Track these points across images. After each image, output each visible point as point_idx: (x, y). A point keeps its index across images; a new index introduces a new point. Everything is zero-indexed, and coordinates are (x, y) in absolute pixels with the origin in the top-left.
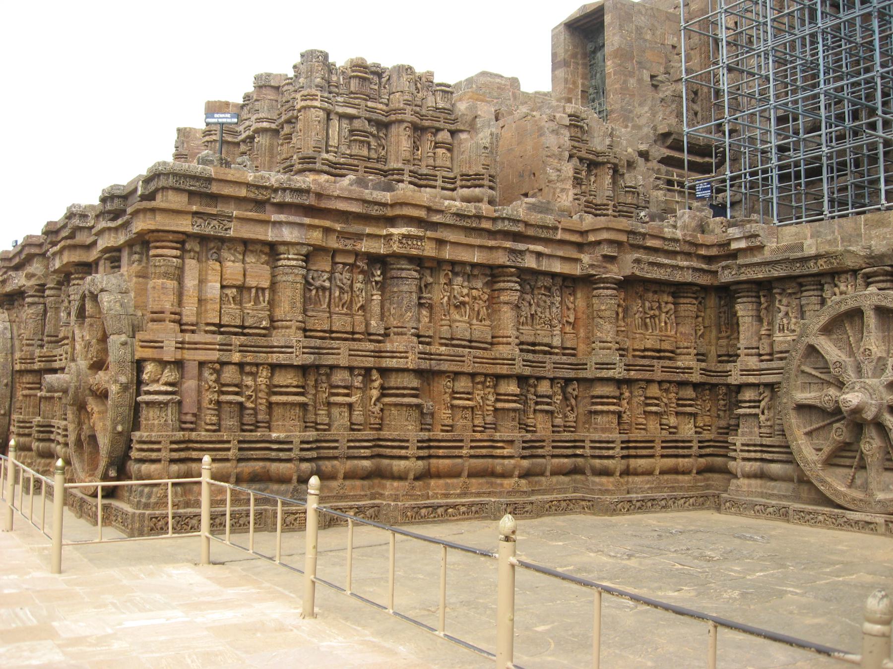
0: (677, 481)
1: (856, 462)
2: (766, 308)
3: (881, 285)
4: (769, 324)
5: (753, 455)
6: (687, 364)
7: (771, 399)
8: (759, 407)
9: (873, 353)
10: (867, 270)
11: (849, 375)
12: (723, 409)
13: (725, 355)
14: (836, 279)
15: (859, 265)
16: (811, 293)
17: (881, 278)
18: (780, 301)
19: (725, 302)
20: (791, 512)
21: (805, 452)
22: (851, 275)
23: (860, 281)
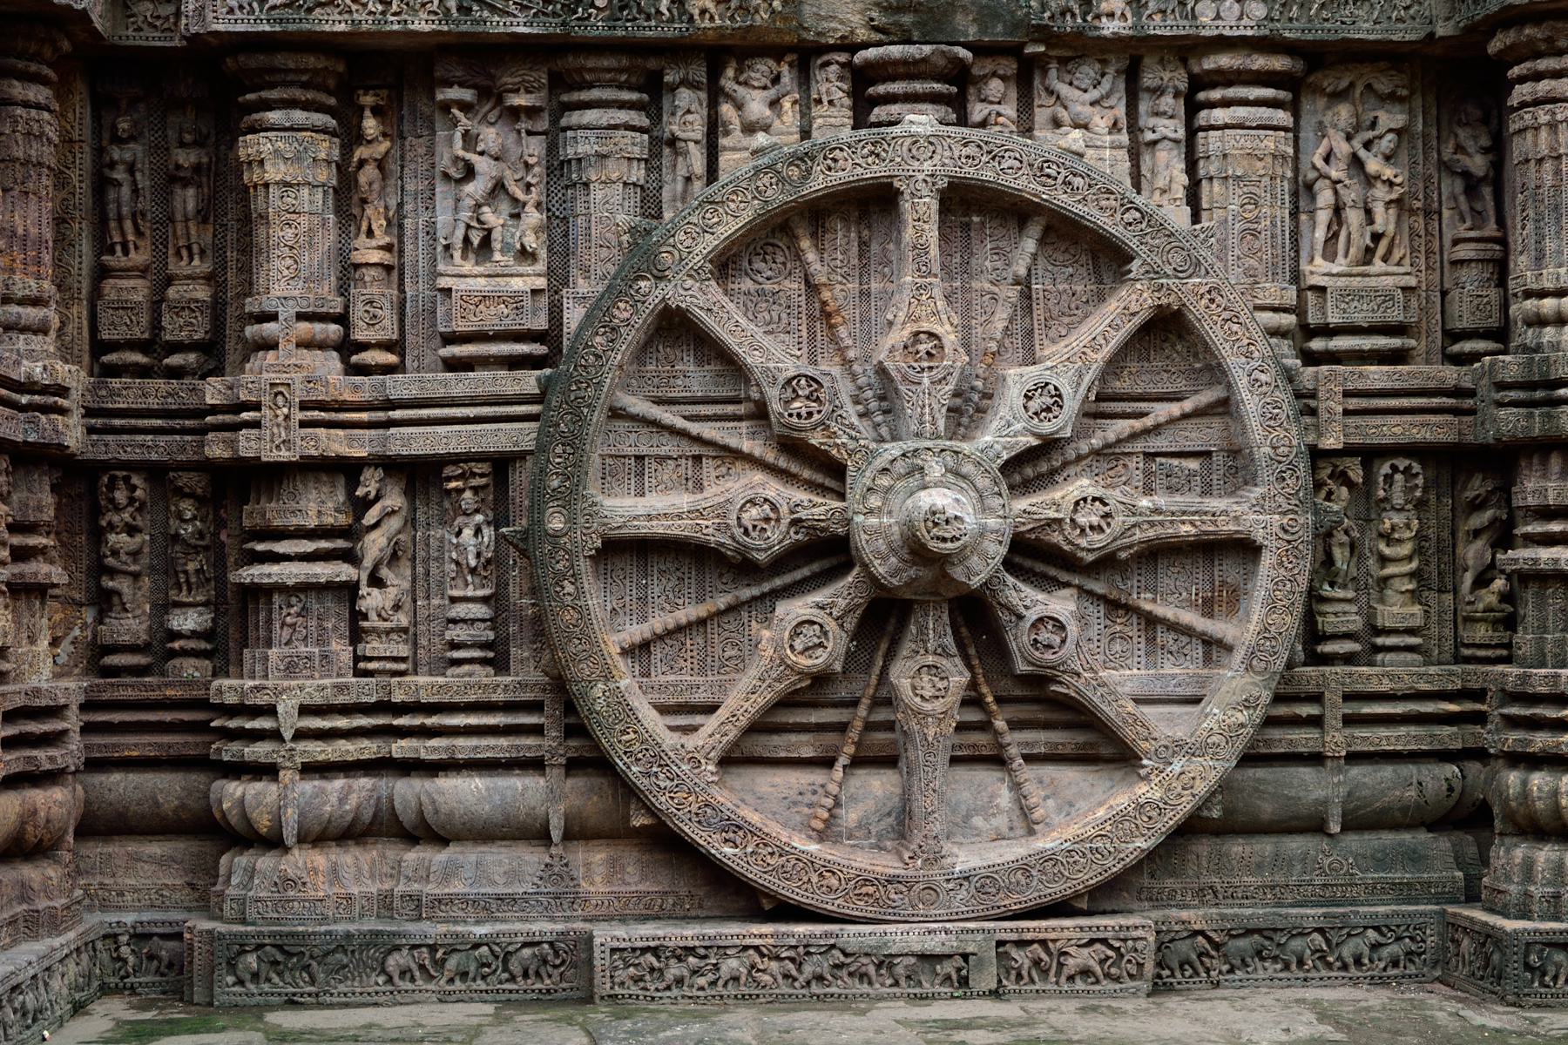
0: (25, 892)
2: (381, 164)
6: (35, 369)
7: (411, 522)
8: (350, 557)
10: (896, 51)
11: (852, 427)
12: (133, 568)
13: (132, 345)
14: (730, 73)
15: (843, 30)
16: (623, 116)
18: (470, 140)
19: (135, 124)
20: (600, 960)
22: (791, 65)
23: (831, 84)
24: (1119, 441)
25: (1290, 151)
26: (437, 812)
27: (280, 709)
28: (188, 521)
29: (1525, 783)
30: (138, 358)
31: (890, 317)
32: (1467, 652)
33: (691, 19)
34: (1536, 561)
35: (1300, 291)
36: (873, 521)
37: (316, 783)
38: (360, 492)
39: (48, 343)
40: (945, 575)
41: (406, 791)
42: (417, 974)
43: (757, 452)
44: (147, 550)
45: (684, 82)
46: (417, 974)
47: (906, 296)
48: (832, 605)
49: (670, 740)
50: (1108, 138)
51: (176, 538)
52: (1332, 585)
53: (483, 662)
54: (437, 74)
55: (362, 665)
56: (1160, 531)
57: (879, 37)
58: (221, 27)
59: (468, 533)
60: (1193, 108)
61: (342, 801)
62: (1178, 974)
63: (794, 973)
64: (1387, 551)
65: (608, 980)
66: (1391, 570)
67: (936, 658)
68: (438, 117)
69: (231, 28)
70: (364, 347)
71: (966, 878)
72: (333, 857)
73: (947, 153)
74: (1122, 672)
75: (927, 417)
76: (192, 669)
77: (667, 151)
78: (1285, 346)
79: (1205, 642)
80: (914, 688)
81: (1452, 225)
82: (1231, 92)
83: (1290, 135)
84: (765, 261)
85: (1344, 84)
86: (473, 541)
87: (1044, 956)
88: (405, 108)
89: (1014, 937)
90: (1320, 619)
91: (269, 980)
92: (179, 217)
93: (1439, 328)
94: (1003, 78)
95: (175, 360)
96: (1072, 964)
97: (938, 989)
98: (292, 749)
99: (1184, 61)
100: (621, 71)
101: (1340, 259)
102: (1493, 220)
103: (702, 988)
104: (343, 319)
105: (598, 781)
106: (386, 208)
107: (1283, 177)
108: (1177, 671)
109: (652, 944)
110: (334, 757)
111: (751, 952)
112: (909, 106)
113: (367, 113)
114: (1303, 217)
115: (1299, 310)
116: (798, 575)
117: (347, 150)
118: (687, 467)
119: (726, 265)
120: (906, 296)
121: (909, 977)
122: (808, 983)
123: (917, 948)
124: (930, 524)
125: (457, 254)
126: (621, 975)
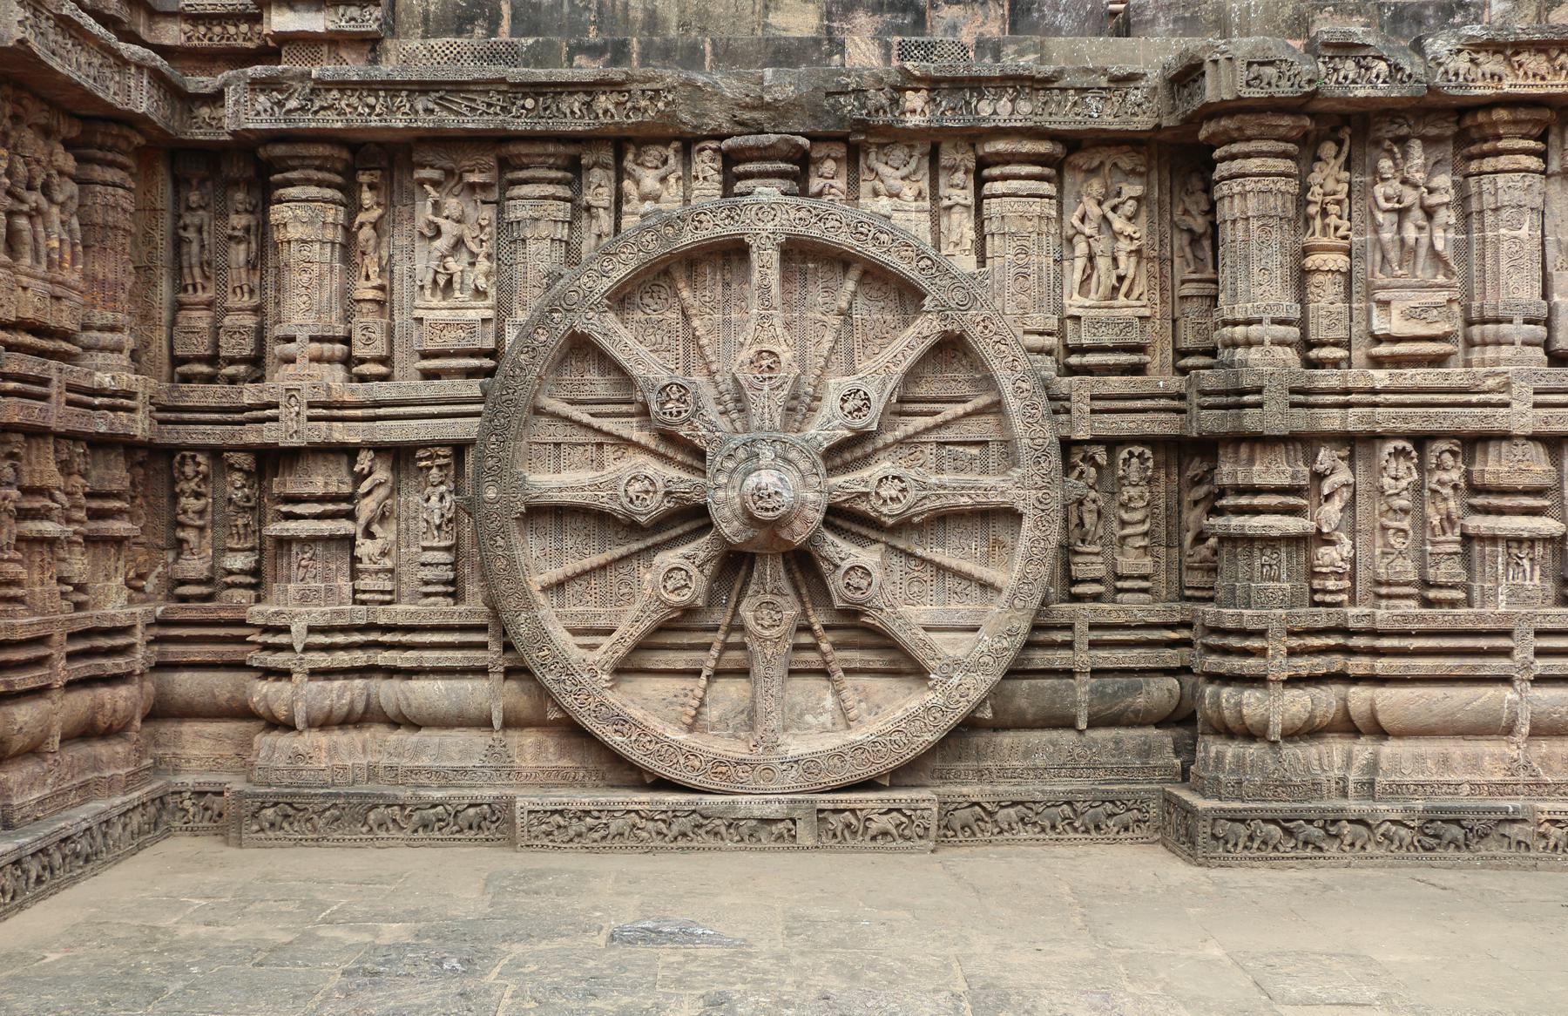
0: (96, 764)
1: (709, 661)
2: (375, 226)
3: (777, 181)
4: (382, 270)
5: (343, 659)
7: (395, 491)
8: (351, 516)
10: (752, 140)
11: (710, 423)
12: (199, 523)
13: (199, 359)
14: (630, 156)
15: (713, 124)
16: (550, 190)
17: (783, 166)
22: (676, 151)
23: (706, 164)
24: (917, 434)
25: (1054, 213)
26: (409, 706)
27: (293, 629)
28: (236, 487)
29: (1217, 696)
30: (204, 369)
31: (742, 339)
32: (1188, 593)
33: (597, 117)
34: (1227, 527)
35: (1061, 321)
36: (721, 494)
37: (320, 683)
38: (357, 468)
39: (124, 359)
40: (776, 535)
41: (388, 692)
42: (391, 826)
43: (643, 442)
44: (210, 509)
45: (596, 164)
46: (391, 826)
47: (752, 325)
48: (695, 556)
49: (576, 654)
50: (914, 204)
51: (230, 500)
52: (1083, 541)
53: (446, 594)
54: (414, 159)
55: (358, 596)
56: (944, 501)
57: (739, 129)
58: (251, 126)
59: (434, 499)
60: (980, 182)
61: (339, 697)
62: (959, 834)
63: (665, 831)
64: (1126, 516)
65: (526, 834)
66: (1129, 531)
67: (773, 597)
68: (417, 190)
69: (258, 126)
70: (363, 361)
71: (796, 762)
72: (335, 738)
73: (785, 216)
74: (918, 607)
75: (767, 416)
76: (241, 596)
77: (585, 215)
78: (1048, 365)
79: (981, 585)
80: (756, 619)
81: (1182, 270)
82: (1008, 169)
83: (1054, 201)
84: (652, 297)
85: (1096, 163)
86: (438, 505)
87: (854, 821)
88: (395, 185)
89: (831, 806)
90: (1073, 567)
91: (281, 828)
92: (233, 266)
93: (1170, 347)
94: (835, 160)
95: (230, 370)
97: (773, 844)
98: (301, 659)
99: (973, 146)
100: (550, 155)
101: (1092, 295)
102: (1210, 266)
103: (596, 841)
104: (347, 341)
105: (528, 684)
106: (380, 258)
107: (1048, 234)
108: (962, 608)
109: (559, 808)
110: (335, 665)
111: (633, 814)
112: (762, 181)
113: (365, 188)
114: (1066, 263)
115: (1061, 333)
116: (674, 533)
117: (351, 216)
119: (621, 299)
120: (752, 325)
121: (751, 835)
122: (676, 838)
123: (757, 813)
124: (756, 498)
125: (428, 292)
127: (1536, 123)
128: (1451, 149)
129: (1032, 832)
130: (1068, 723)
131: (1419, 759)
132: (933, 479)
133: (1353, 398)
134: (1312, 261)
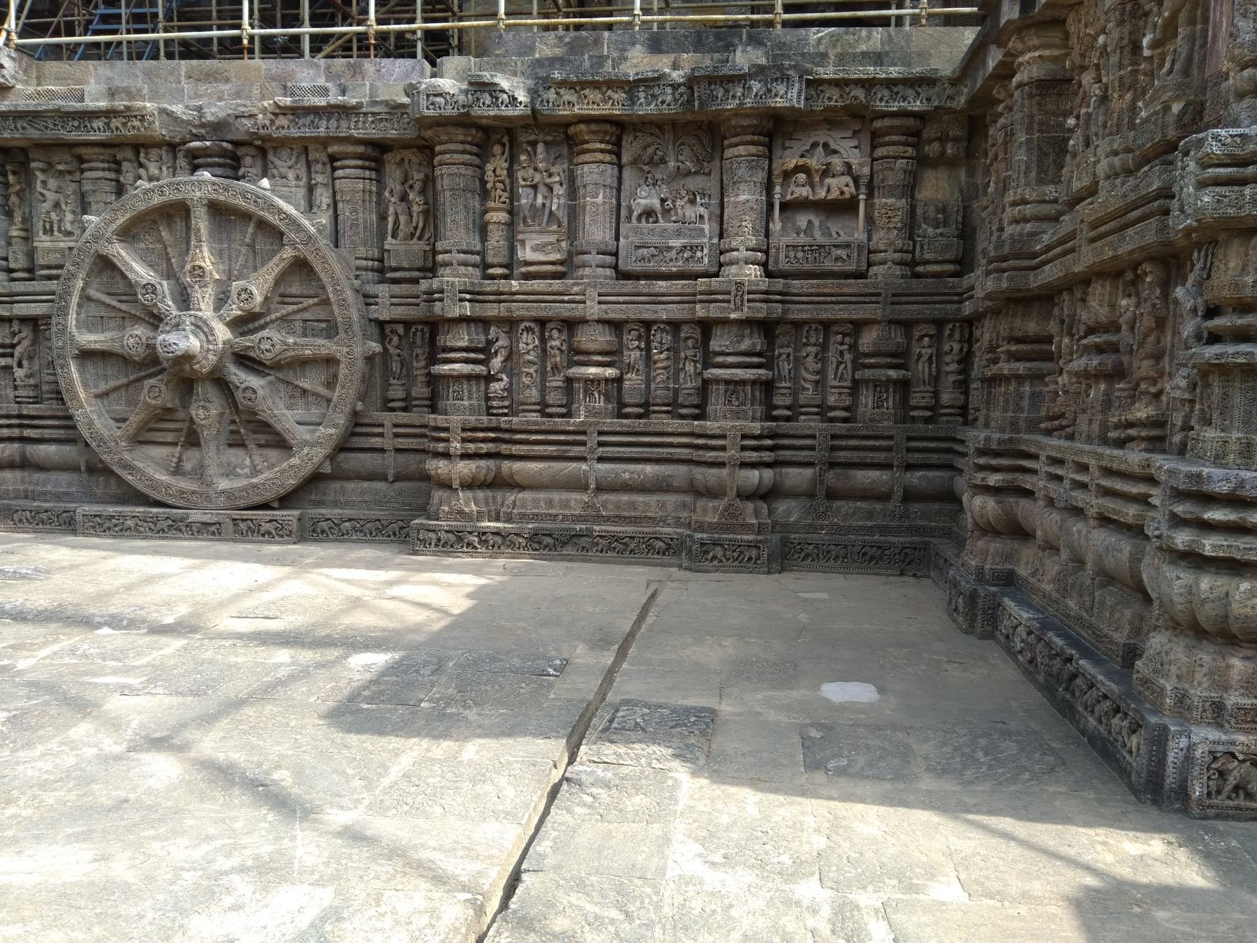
7: (34, 343)
9: (207, 273)
10: (197, 144)
14: (142, 155)
16: (100, 174)
17: (217, 160)
20: (79, 518)
21: (99, 426)
23: (182, 162)
24: (289, 314)
45: (125, 160)
66: (418, 372)
85: (398, 159)
94: (253, 157)
96: (263, 529)
108: (315, 412)
118: (119, 322)
126: (87, 525)
127: (605, 133)
128: (566, 149)
129: (360, 536)
130: (384, 478)
131: (536, 501)
132: (291, 341)
133: (502, 297)
134: (488, 216)
